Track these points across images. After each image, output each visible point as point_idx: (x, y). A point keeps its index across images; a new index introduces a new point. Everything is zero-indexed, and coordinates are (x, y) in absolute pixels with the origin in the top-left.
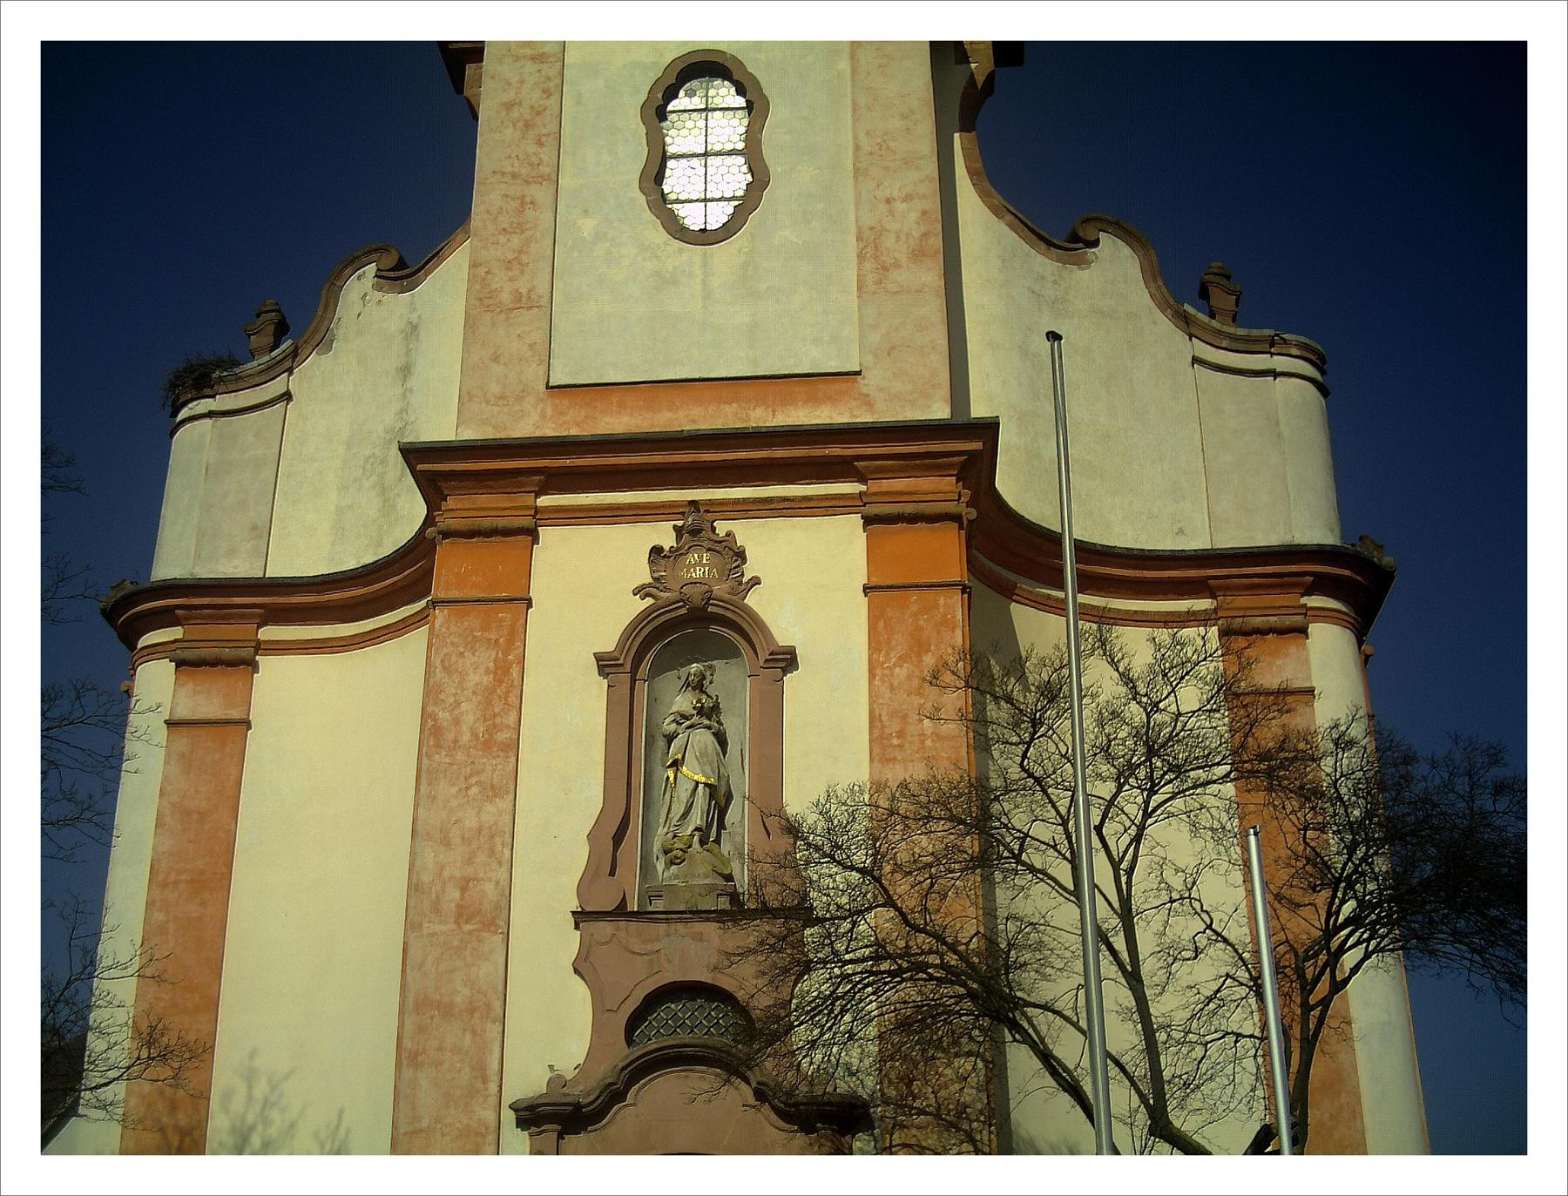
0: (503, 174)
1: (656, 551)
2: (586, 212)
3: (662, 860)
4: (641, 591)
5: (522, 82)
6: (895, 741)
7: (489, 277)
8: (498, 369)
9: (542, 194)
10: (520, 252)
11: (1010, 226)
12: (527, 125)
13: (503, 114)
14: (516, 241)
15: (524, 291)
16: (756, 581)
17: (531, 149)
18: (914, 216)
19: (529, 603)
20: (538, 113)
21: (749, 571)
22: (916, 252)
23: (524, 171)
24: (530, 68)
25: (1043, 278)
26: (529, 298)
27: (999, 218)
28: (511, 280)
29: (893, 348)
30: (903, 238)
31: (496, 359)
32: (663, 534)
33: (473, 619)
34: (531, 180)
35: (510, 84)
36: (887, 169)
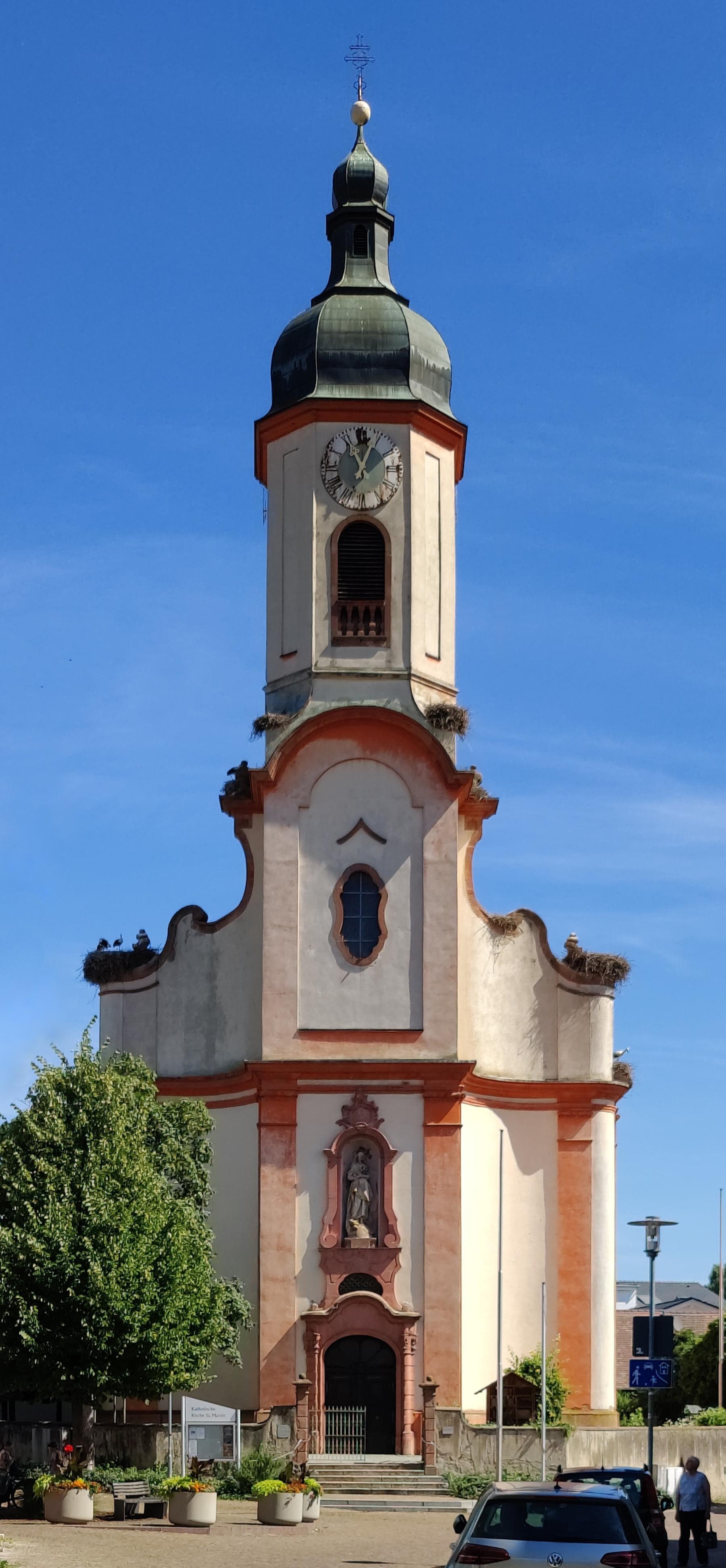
0: (275, 926)
1: (344, 1108)
3: (349, 1227)
4: (339, 1123)
6: (434, 1187)
16: (382, 1120)
19: (295, 1125)
21: (381, 1115)
31: (276, 1017)
32: (345, 1098)
33: (276, 1133)
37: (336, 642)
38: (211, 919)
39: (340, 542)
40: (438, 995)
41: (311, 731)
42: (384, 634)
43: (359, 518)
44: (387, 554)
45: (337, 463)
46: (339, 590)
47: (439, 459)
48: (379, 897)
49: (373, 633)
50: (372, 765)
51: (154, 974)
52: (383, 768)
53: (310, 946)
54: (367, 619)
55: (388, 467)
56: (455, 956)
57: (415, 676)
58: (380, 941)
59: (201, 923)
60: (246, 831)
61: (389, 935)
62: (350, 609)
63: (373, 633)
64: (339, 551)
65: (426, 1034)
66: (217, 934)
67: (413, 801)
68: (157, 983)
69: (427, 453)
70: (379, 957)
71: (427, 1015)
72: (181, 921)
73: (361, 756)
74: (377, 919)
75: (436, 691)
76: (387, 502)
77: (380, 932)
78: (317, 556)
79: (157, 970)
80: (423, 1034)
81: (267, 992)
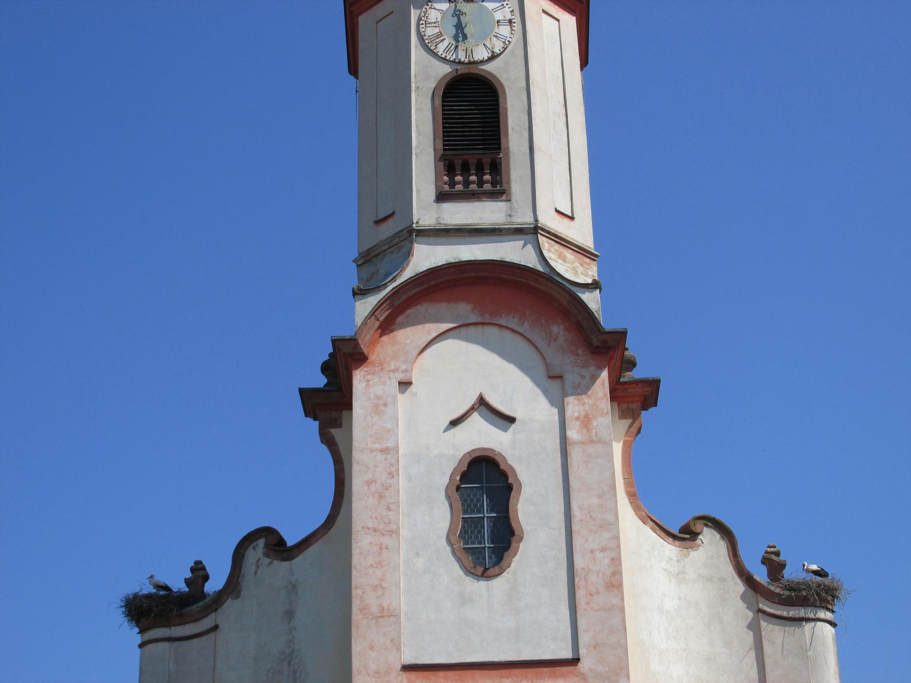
0: (368, 529)
2: (417, 554)
5: (376, 466)
7: (365, 595)
8: (373, 654)
9: (387, 541)
10: (381, 580)
11: (652, 529)
12: (381, 497)
13: (366, 488)
14: (378, 572)
15: (385, 605)
17: (384, 513)
18: (607, 561)
20: (387, 489)
22: (608, 585)
23: (381, 527)
24: (380, 457)
25: (671, 559)
26: (388, 610)
27: (645, 524)
28: (377, 598)
29: (597, 644)
30: (601, 575)
31: (372, 648)
34: (385, 533)
35: (369, 468)
36: (591, 531)
37: (442, 197)
38: (291, 541)
39: (443, 97)
40: (598, 610)
41: (414, 292)
42: (501, 186)
43: (466, 71)
44: (501, 105)
45: (439, 20)
46: (444, 145)
47: (558, 20)
48: (509, 488)
49: (487, 187)
50: (494, 330)
51: (213, 615)
52: (508, 334)
53: (417, 554)
54: (480, 171)
55: (498, 22)
56: (616, 561)
57: (543, 229)
58: (513, 545)
59: (277, 548)
60: (334, 431)
61: (525, 536)
62: (458, 162)
63: (487, 187)
64: (443, 106)
65: (585, 664)
66: (299, 560)
67: (548, 366)
68: (216, 628)
69: (544, 11)
70: (513, 565)
71: (584, 639)
72: (251, 547)
73: (479, 320)
74: (507, 518)
75: (571, 251)
76: (499, 55)
77: (512, 533)
78: (417, 109)
79: (216, 610)
80: (579, 664)
81: (356, 615)
